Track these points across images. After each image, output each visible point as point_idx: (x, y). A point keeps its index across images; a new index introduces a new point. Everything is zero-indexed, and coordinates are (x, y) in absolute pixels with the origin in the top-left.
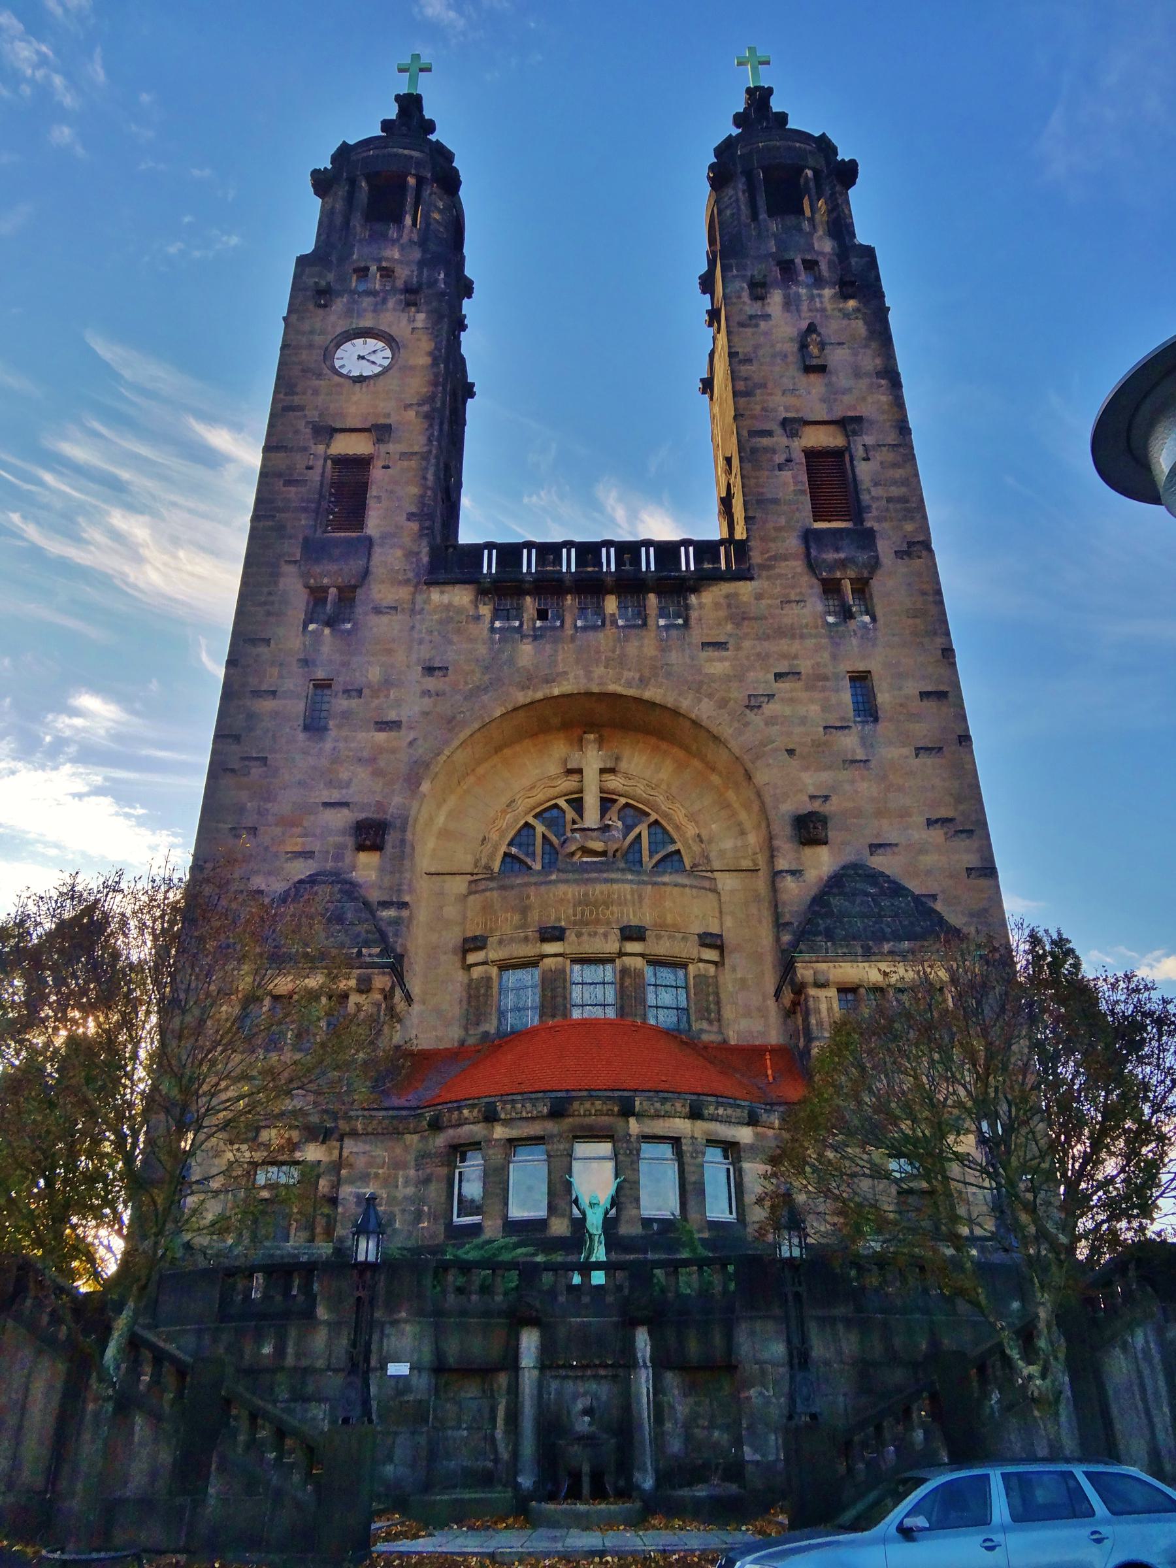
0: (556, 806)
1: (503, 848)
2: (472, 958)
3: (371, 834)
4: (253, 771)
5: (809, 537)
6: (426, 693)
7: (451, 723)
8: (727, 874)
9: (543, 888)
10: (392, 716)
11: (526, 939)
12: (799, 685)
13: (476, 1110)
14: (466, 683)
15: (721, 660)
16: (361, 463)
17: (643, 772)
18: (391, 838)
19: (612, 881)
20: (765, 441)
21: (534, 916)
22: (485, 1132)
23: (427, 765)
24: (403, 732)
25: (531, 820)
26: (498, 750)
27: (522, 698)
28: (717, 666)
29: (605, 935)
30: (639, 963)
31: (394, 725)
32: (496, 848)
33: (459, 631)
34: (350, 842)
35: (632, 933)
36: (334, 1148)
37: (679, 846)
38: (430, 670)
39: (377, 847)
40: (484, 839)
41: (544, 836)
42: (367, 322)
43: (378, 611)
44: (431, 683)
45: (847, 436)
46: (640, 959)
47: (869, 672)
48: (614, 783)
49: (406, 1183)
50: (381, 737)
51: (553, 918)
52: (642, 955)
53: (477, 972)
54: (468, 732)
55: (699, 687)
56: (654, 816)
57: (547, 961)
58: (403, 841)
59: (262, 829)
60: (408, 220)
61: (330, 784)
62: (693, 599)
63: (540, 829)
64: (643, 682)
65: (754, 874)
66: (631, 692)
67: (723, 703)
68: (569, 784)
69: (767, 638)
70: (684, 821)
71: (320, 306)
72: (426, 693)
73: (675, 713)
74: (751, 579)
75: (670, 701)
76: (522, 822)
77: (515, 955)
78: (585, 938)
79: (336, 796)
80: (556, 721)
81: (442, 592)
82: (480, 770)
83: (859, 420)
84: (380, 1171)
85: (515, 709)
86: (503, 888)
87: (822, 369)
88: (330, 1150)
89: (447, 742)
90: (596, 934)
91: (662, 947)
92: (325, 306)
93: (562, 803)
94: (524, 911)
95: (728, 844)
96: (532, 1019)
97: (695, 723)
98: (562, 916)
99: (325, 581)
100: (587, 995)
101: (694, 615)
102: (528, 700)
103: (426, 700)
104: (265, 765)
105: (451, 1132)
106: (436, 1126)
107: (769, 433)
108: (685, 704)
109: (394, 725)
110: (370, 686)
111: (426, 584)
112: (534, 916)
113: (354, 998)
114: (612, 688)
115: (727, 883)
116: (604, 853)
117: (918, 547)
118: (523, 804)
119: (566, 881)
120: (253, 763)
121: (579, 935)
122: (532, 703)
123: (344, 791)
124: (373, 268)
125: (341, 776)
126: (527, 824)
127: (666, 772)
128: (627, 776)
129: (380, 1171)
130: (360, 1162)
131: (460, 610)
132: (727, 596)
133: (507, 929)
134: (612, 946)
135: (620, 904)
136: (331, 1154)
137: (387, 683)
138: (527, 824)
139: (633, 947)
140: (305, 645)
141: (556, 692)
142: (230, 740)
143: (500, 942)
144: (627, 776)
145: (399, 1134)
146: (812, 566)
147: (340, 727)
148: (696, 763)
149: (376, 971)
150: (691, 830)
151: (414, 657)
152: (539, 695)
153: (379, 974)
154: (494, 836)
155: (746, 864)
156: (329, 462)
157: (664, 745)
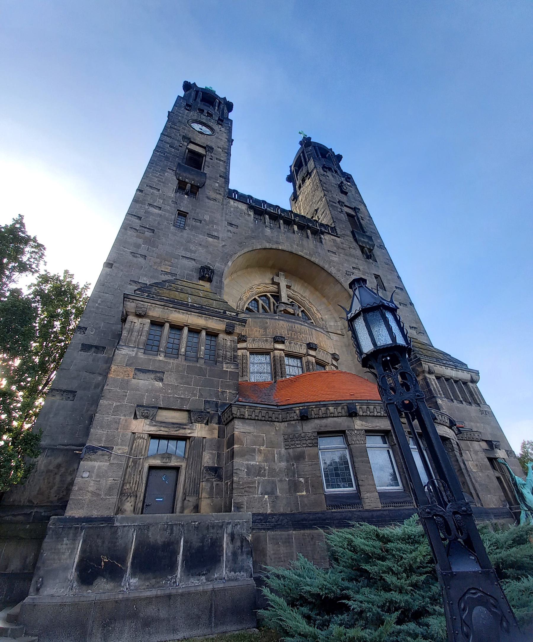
0: (265, 296)
1: (246, 306)
2: (240, 346)
3: (206, 274)
4: (146, 233)
5: (353, 232)
6: (228, 231)
7: (241, 244)
8: (333, 334)
9: (273, 320)
10: (215, 234)
11: (267, 340)
12: (361, 273)
13: (340, 408)
14: (245, 233)
15: (336, 257)
16: (200, 156)
17: (301, 292)
18: (215, 278)
19: (301, 324)
20: (334, 204)
21: (270, 332)
22: (346, 424)
23: (231, 256)
24: (220, 241)
25: (257, 298)
26: (247, 267)
27: (268, 246)
28: (335, 258)
29: (301, 345)
30: (313, 360)
31: (217, 238)
32: (245, 303)
33: (241, 216)
34: (196, 275)
35: (311, 346)
36: (214, 429)
37: (313, 321)
38: (231, 224)
39: (210, 280)
40: (241, 299)
41: (263, 306)
42: (204, 121)
43: (208, 198)
44: (230, 228)
45: (356, 213)
46: (314, 358)
47: (379, 276)
48: (290, 292)
49: (281, 459)
50: (210, 239)
51: (279, 333)
52: (314, 357)
53: (240, 353)
54: (246, 250)
55: (330, 262)
56: (302, 309)
57: (276, 352)
58: (221, 282)
59: (148, 257)
60: (217, 108)
61: (186, 249)
62: (322, 236)
63: (261, 302)
64: (311, 255)
65: (342, 337)
66: (307, 257)
67: (339, 270)
68: (273, 288)
69: (347, 255)
70: (316, 312)
71: (187, 109)
72: (228, 231)
73: (323, 269)
74: (339, 237)
75: (321, 264)
76: (253, 298)
77: (261, 347)
78: (292, 345)
79: (188, 255)
80: (271, 263)
81: (234, 202)
82: (239, 273)
83: (359, 209)
84: (262, 448)
85: (265, 249)
86: (255, 318)
87: (346, 193)
88: (211, 430)
89: (239, 251)
90: (297, 344)
91: (321, 356)
92: (188, 110)
93: (268, 294)
94: (265, 329)
95: (332, 324)
96: (268, 378)
97: (330, 274)
98: (284, 333)
99: (187, 180)
100: (291, 370)
101: (323, 241)
102: (270, 247)
103: (229, 233)
104: (153, 233)
105: (317, 421)
106: (304, 417)
107: (335, 203)
108: (326, 267)
109: (217, 238)
110: (205, 220)
111: (228, 197)
112: (270, 331)
113: (221, 336)
114: (300, 253)
115: (334, 337)
116: (294, 314)
117: (382, 246)
118: (255, 290)
119: (282, 320)
120: (146, 230)
121: (290, 343)
122: (271, 249)
123: (193, 254)
124: (205, 111)
125: (191, 248)
126: (255, 299)
127: (307, 294)
128: (293, 290)
129: (262, 448)
130: (247, 440)
131: (242, 210)
132: (333, 240)
133: (257, 334)
134: (303, 351)
135: (305, 334)
136: (213, 433)
137: (212, 222)
138: (255, 299)
139: (311, 352)
140: (176, 197)
141: (280, 248)
142: (136, 218)
143: (254, 340)
144: (293, 290)
145: (271, 421)
146: (356, 240)
147: (191, 230)
148: (317, 293)
149: (238, 323)
150: (319, 316)
151: (224, 219)
152: (274, 247)
153: (239, 325)
154: (245, 299)
155: (339, 332)
156: (187, 150)
157: (306, 284)
